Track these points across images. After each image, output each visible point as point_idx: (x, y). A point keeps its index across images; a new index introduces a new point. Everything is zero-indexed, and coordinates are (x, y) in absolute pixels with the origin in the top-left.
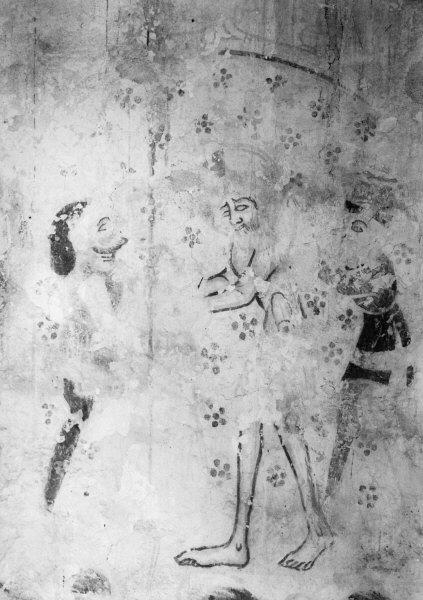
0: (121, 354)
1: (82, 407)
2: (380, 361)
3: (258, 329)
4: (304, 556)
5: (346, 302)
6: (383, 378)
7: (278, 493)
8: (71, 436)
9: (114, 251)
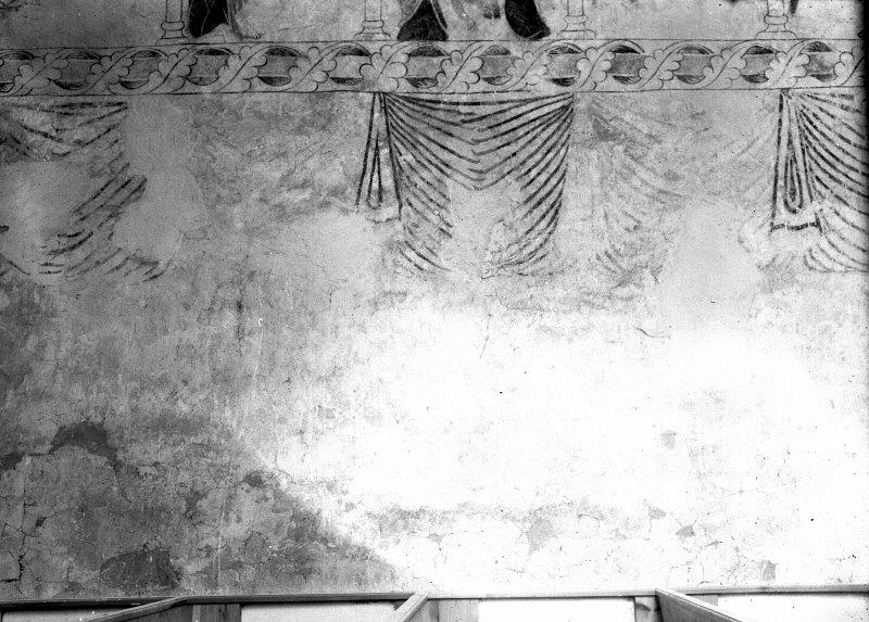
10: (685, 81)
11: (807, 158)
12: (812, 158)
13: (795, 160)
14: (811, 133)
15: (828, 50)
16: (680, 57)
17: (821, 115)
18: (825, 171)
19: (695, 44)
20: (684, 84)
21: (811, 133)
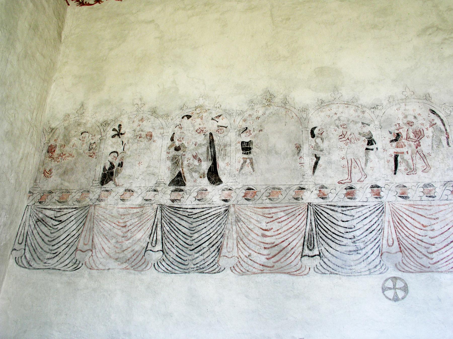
0: (324, 149)
1: (318, 158)
2: (370, 147)
3: (349, 144)
4: (362, 180)
5: (364, 138)
6: (372, 150)
7: (356, 170)
8: (316, 163)
10: (271, 200)
11: (317, 229)
13: (312, 230)
14: (319, 220)
15: (326, 188)
16: (270, 191)
17: (323, 212)
18: (324, 235)
19: (276, 186)
20: (271, 201)
21: (319, 220)
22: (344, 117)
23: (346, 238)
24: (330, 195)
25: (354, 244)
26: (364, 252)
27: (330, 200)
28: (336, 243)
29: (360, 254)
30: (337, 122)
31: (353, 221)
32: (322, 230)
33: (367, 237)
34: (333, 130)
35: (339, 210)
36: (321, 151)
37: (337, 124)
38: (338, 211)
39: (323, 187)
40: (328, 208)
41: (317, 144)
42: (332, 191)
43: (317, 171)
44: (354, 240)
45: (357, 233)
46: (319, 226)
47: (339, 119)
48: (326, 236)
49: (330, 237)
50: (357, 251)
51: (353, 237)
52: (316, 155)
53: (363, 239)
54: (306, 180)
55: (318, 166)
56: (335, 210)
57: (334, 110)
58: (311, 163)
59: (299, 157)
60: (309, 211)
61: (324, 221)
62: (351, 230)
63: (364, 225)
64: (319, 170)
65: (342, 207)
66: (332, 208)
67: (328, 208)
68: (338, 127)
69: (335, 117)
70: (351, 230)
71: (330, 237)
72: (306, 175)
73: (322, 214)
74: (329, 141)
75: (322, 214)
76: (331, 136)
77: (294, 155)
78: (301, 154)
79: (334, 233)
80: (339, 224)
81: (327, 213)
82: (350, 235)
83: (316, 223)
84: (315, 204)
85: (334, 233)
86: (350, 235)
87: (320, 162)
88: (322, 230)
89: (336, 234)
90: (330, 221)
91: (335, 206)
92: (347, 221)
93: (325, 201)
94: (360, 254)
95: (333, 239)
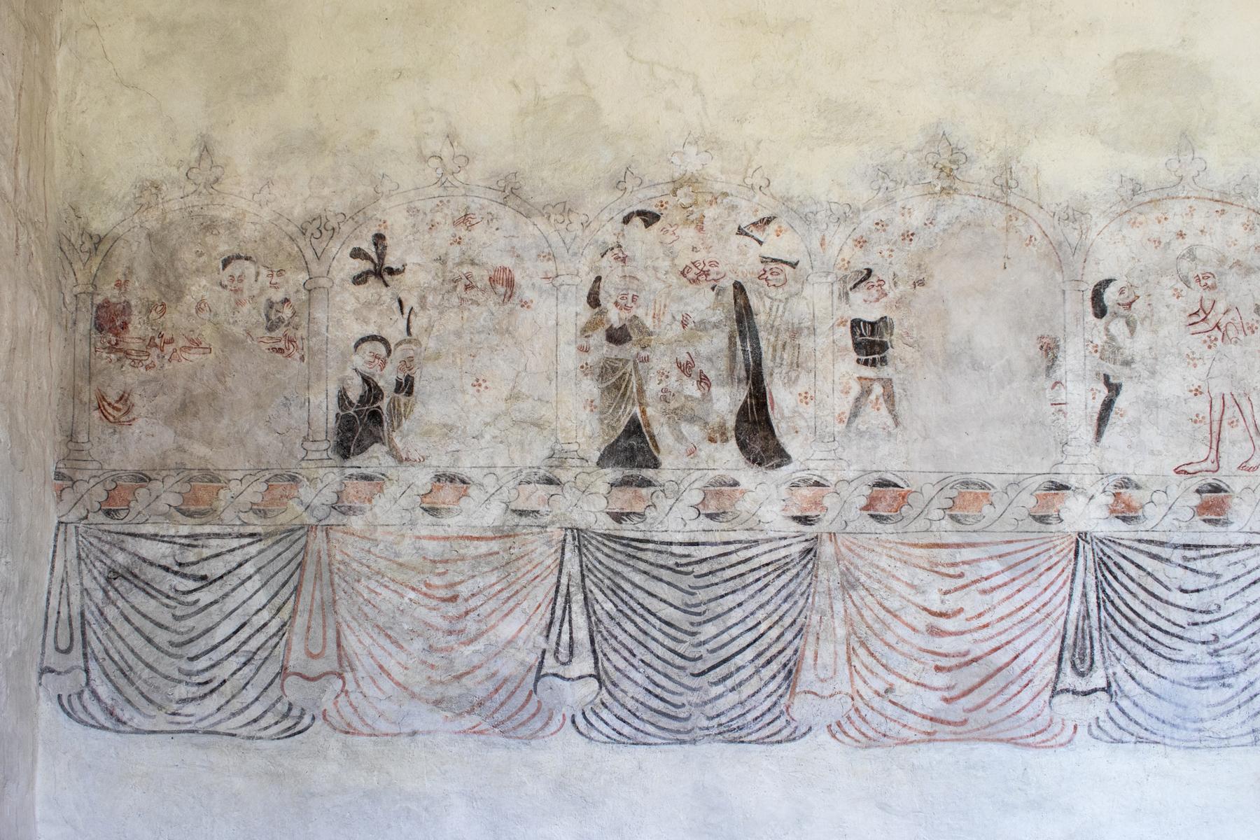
0: (1137, 358)
1: (1114, 389)
8: (1108, 405)
9: (1130, 304)
10: (959, 521)
11: (1103, 613)
12: (1109, 614)
13: (1087, 616)
14: (1109, 585)
15: (1137, 487)
16: (954, 493)
18: (1124, 630)
19: (974, 477)
20: (958, 525)
21: (1109, 585)
22: (1209, 247)
23: (1190, 641)
24: (1149, 509)
25: (1216, 659)
26: (1243, 680)
27: (1150, 524)
28: (1160, 655)
29: (1229, 686)
30: (1185, 265)
31: (1214, 591)
32: (1118, 616)
33: (1254, 639)
34: (1170, 292)
35: (1177, 555)
36: (1127, 363)
37: (1184, 272)
38: (1173, 559)
39: (1126, 483)
40: (1141, 551)
41: (1112, 338)
42: (1156, 497)
43: (1110, 433)
44: (1217, 646)
45: (1227, 626)
46: (1108, 605)
47: (1191, 254)
48: (1129, 635)
49: (1143, 638)
50: (1220, 679)
51: (1212, 638)
52: (1106, 378)
53: (1243, 645)
54: (1071, 460)
55: (1112, 414)
56: (1164, 555)
57: (1175, 223)
58: (1091, 403)
59: (1049, 384)
60: (1081, 559)
61: (1126, 588)
62: (1207, 618)
63: (1249, 604)
64: (1118, 429)
65: (1187, 546)
66: (1155, 550)
67: (1141, 551)
68: (1187, 283)
69: (1179, 247)
70: (1207, 618)
71: (1143, 638)
72: (1073, 443)
73: (1120, 568)
74: (1155, 332)
75: (1120, 568)
76: (1164, 312)
77: (1034, 376)
78: (1059, 373)
79: (1153, 626)
80: (1171, 600)
81: (1138, 566)
82: (1206, 633)
83: (1101, 595)
84: (1100, 535)
85: (1153, 626)
86: (1206, 633)
87: (1121, 402)
88: (1118, 616)
89: (1160, 629)
90: (1146, 590)
91: (1162, 544)
92: (1198, 591)
93: (1131, 527)
94: (1229, 686)
95: (1151, 644)
